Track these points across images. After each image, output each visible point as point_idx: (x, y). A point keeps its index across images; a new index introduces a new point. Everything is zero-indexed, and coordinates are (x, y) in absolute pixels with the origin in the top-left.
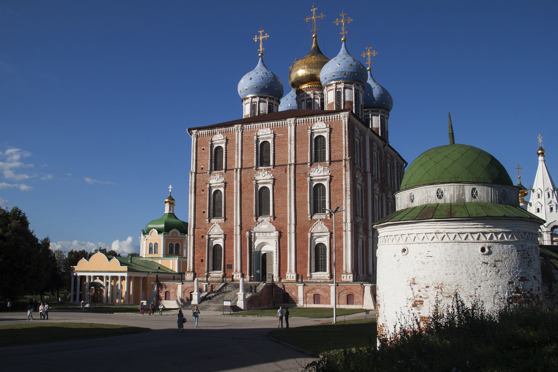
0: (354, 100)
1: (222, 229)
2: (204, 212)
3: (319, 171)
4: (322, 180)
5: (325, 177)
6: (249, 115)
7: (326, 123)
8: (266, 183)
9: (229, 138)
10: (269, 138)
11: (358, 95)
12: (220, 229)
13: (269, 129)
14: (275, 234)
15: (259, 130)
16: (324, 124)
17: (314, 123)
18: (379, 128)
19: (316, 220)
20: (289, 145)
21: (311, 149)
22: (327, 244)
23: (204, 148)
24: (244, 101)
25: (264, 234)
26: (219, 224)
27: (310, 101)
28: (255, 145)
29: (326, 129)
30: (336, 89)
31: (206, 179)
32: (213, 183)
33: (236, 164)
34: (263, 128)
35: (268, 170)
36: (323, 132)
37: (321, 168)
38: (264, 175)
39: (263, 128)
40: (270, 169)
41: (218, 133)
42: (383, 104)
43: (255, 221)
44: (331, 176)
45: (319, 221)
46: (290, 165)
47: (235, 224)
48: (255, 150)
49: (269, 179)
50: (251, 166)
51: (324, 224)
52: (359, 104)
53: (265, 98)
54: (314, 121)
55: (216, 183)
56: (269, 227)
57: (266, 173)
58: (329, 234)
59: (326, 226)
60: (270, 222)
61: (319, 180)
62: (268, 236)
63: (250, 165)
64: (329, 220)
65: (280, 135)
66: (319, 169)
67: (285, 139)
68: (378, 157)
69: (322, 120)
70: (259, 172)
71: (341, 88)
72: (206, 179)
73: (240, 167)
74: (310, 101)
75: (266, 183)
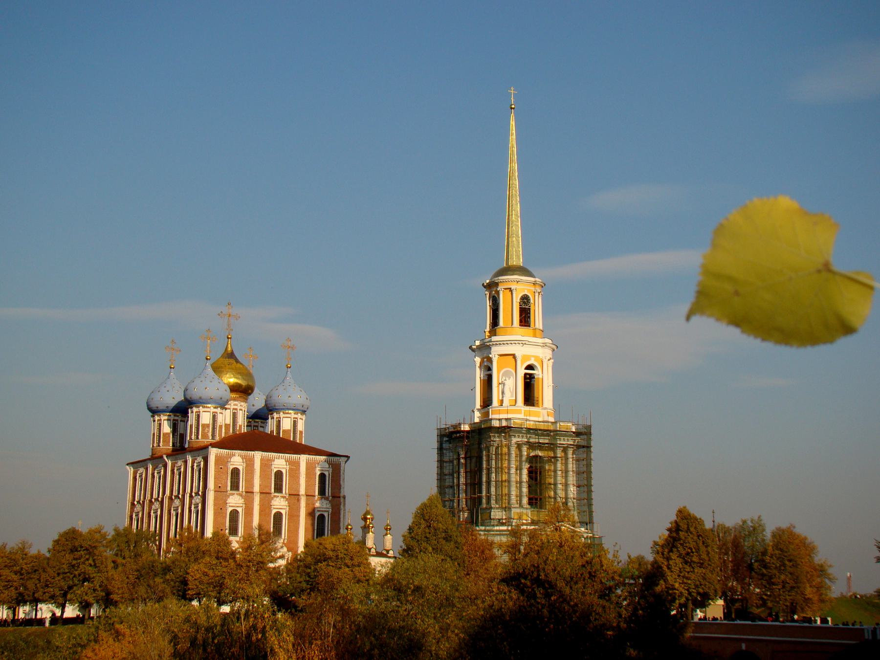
5: (328, 510)
6: (211, 425)
7: (329, 464)
8: (282, 509)
13: (284, 460)
15: (276, 460)
24: (201, 408)
27: (236, 411)
29: (328, 469)
31: (224, 498)
34: (279, 459)
36: (326, 470)
39: (279, 459)
41: (237, 455)
46: (302, 495)
49: (284, 506)
50: (268, 492)
55: (236, 504)
61: (322, 511)
63: (267, 490)
67: (297, 472)
71: (297, 418)
72: (224, 498)
74: (236, 411)
75: (282, 509)
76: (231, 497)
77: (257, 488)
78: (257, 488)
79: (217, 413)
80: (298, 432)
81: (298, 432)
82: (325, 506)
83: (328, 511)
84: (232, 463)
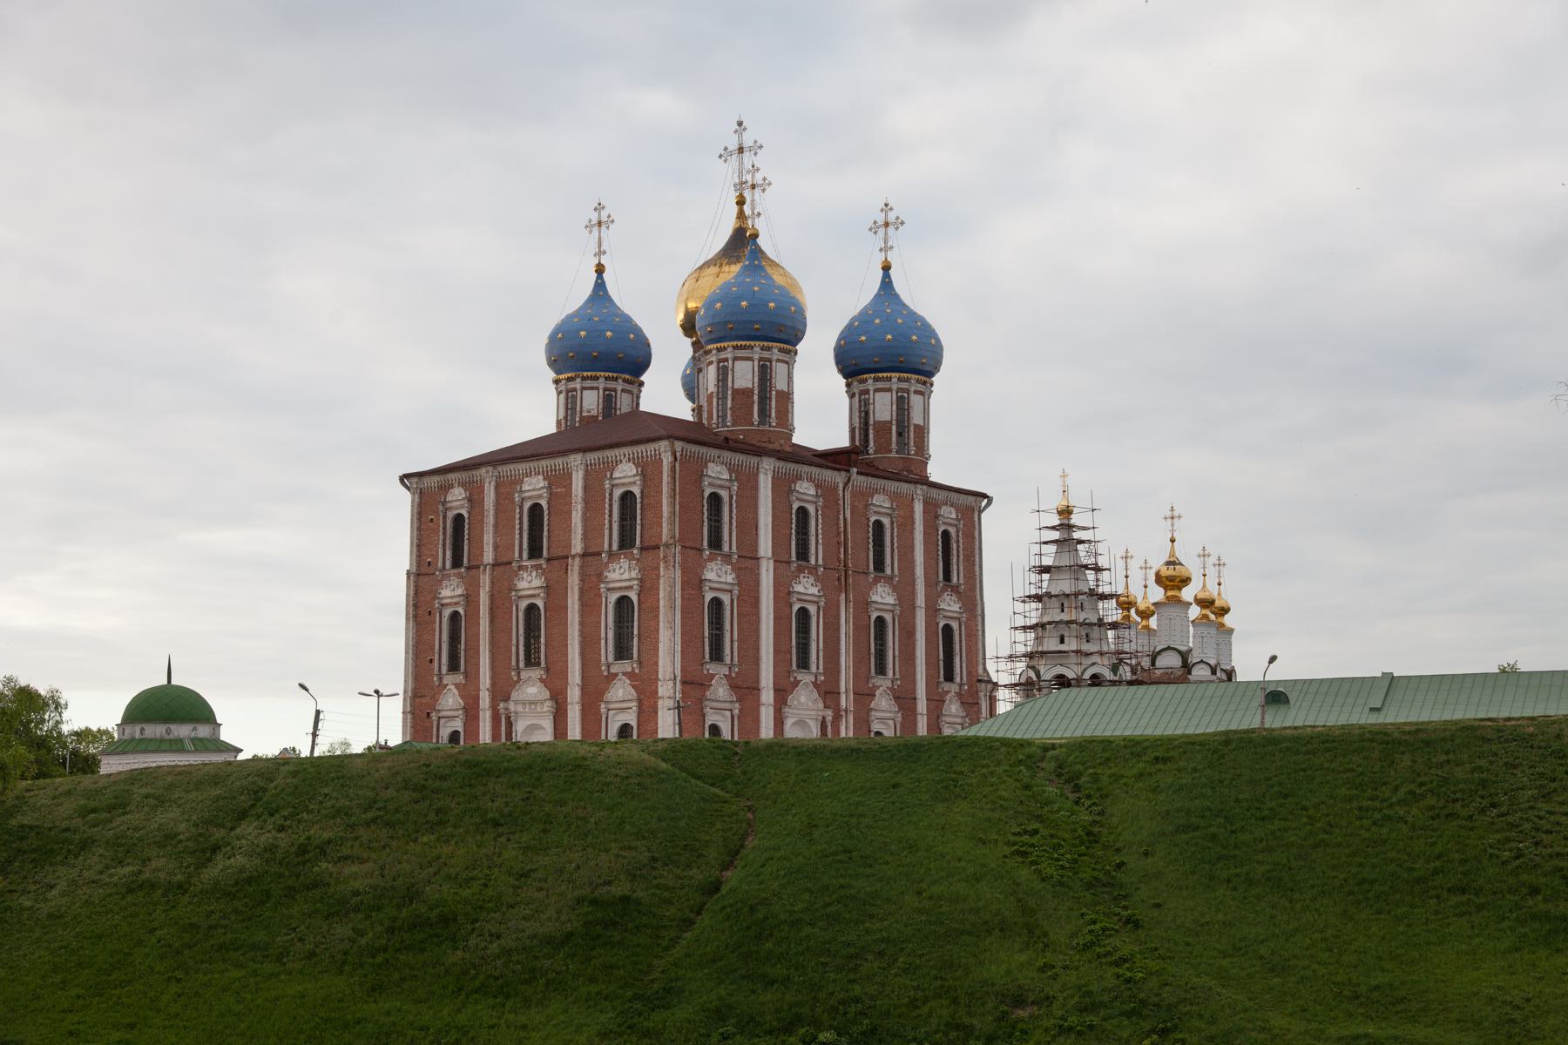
0: (756, 385)
1: (462, 697)
2: (431, 661)
3: (622, 571)
4: (626, 588)
9: (476, 497)
10: (540, 496)
11: (769, 371)
12: (459, 698)
13: (541, 477)
14: (548, 706)
15: (525, 479)
16: (633, 466)
17: (617, 465)
18: (891, 422)
19: (617, 675)
20: (574, 513)
21: (610, 522)
22: (634, 723)
23: (433, 517)
25: (533, 706)
26: (457, 686)
28: (518, 511)
30: (719, 361)
32: (446, 598)
33: (485, 554)
34: (531, 476)
35: (537, 567)
36: (630, 483)
37: (624, 563)
38: (529, 578)
39: (531, 476)
40: (541, 565)
42: (901, 362)
43: (515, 679)
44: (641, 581)
45: (620, 676)
46: (574, 557)
47: (481, 687)
48: (517, 522)
51: (631, 684)
52: (770, 392)
53: (596, 378)
54: (617, 462)
56: (539, 692)
57: (534, 574)
58: (634, 704)
59: (633, 687)
60: (541, 680)
61: (621, 588)
62: (539, 710)
64: (637, 674)
65: (559, 490)
66: (622, 564)
68: (820, 512)
69: (629, 459)
70: (522, 572)
73: (491, 561)
76: (445, 583)
77: (488, 556)
78: (488, 556)
79: (575, 390)
80: (730, 392)
81: (730, 392)
82: (626, 576)
83: (631, 587)
84: (449, 505)
